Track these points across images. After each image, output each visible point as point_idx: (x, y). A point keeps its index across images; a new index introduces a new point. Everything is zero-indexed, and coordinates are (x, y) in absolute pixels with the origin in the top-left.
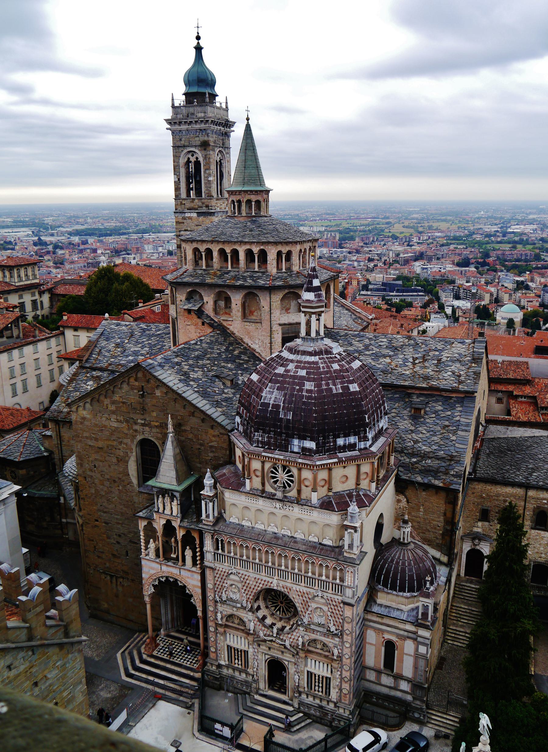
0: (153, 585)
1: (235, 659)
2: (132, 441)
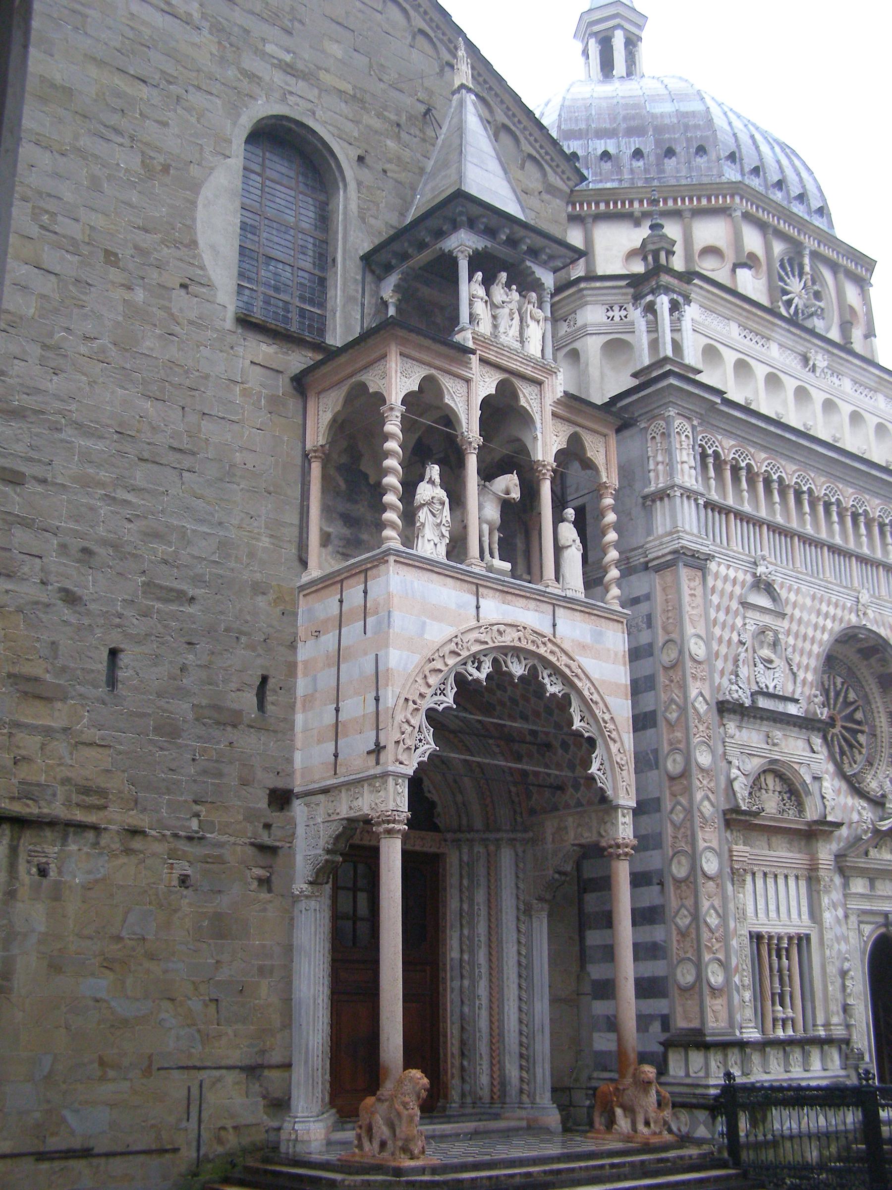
1: (773, 1004)
2: (234, 111)
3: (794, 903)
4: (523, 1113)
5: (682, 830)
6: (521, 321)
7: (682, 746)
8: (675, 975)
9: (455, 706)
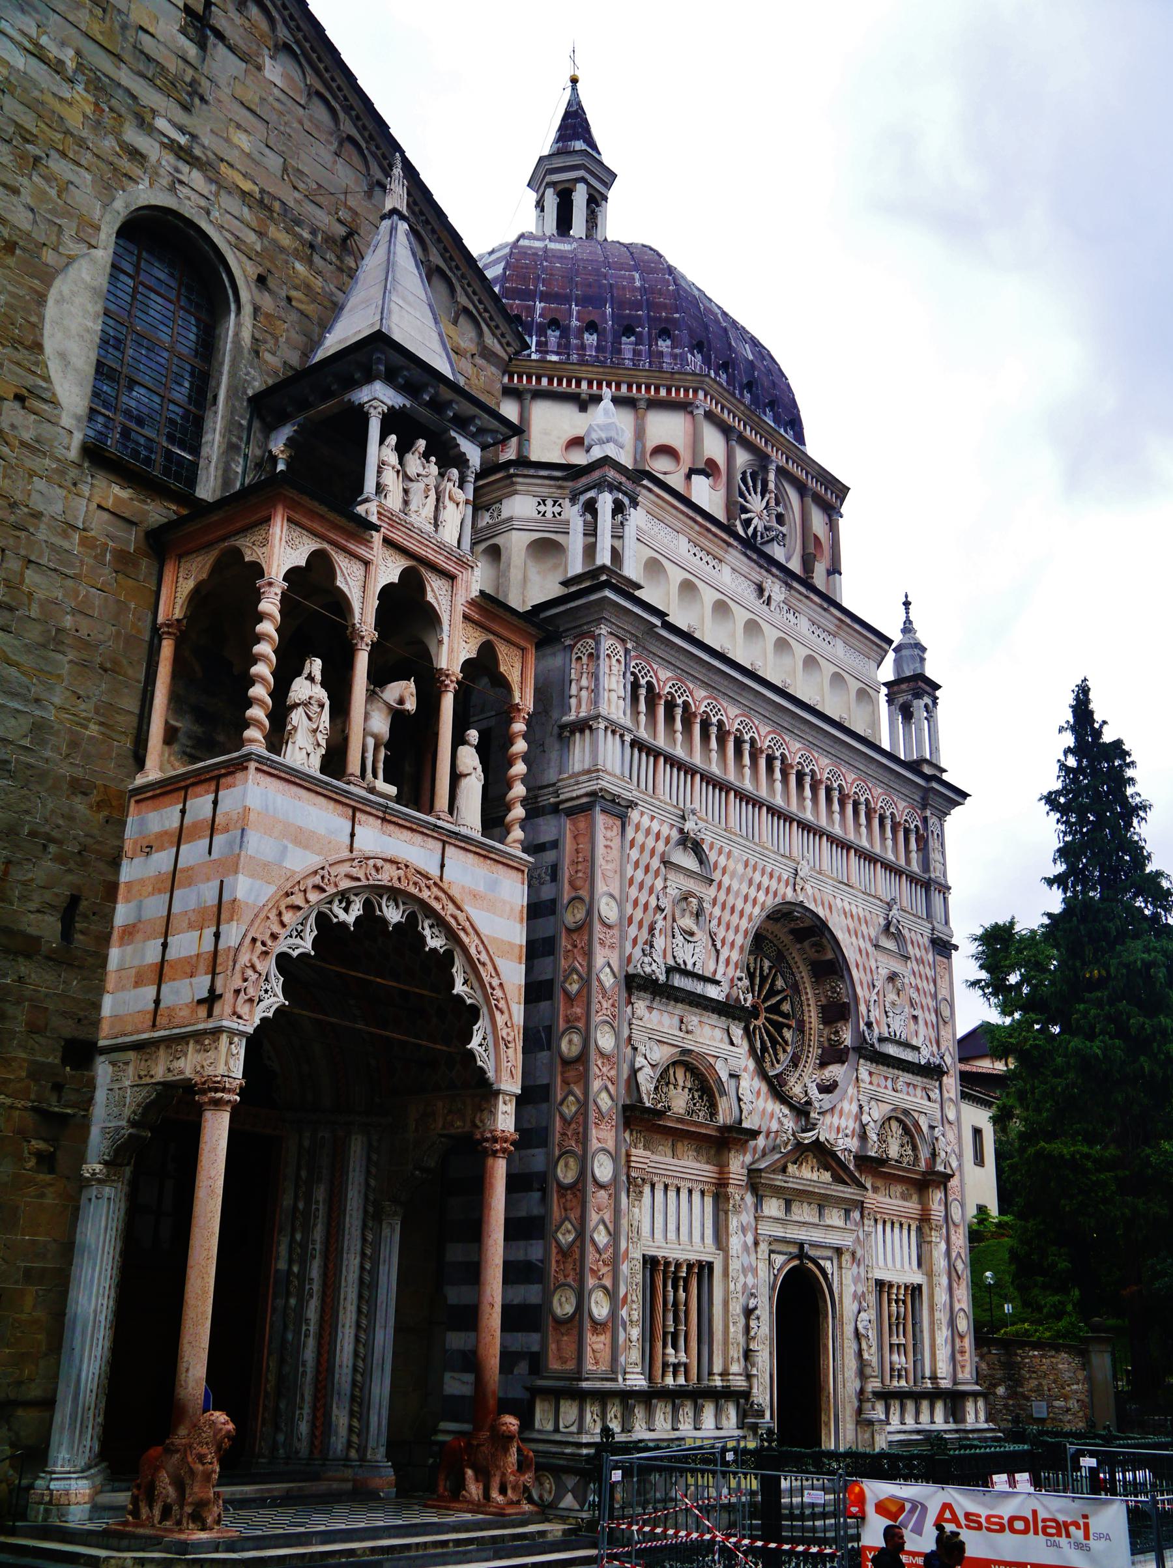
0: (283, 960)
1: (665, 1346)
3: (696, 1224)
4: (349, 1473)
5: (573, 1126)
6: (438, 500)
7: (580, 1025)
8: (551, 1303)
9: (313, 953)
